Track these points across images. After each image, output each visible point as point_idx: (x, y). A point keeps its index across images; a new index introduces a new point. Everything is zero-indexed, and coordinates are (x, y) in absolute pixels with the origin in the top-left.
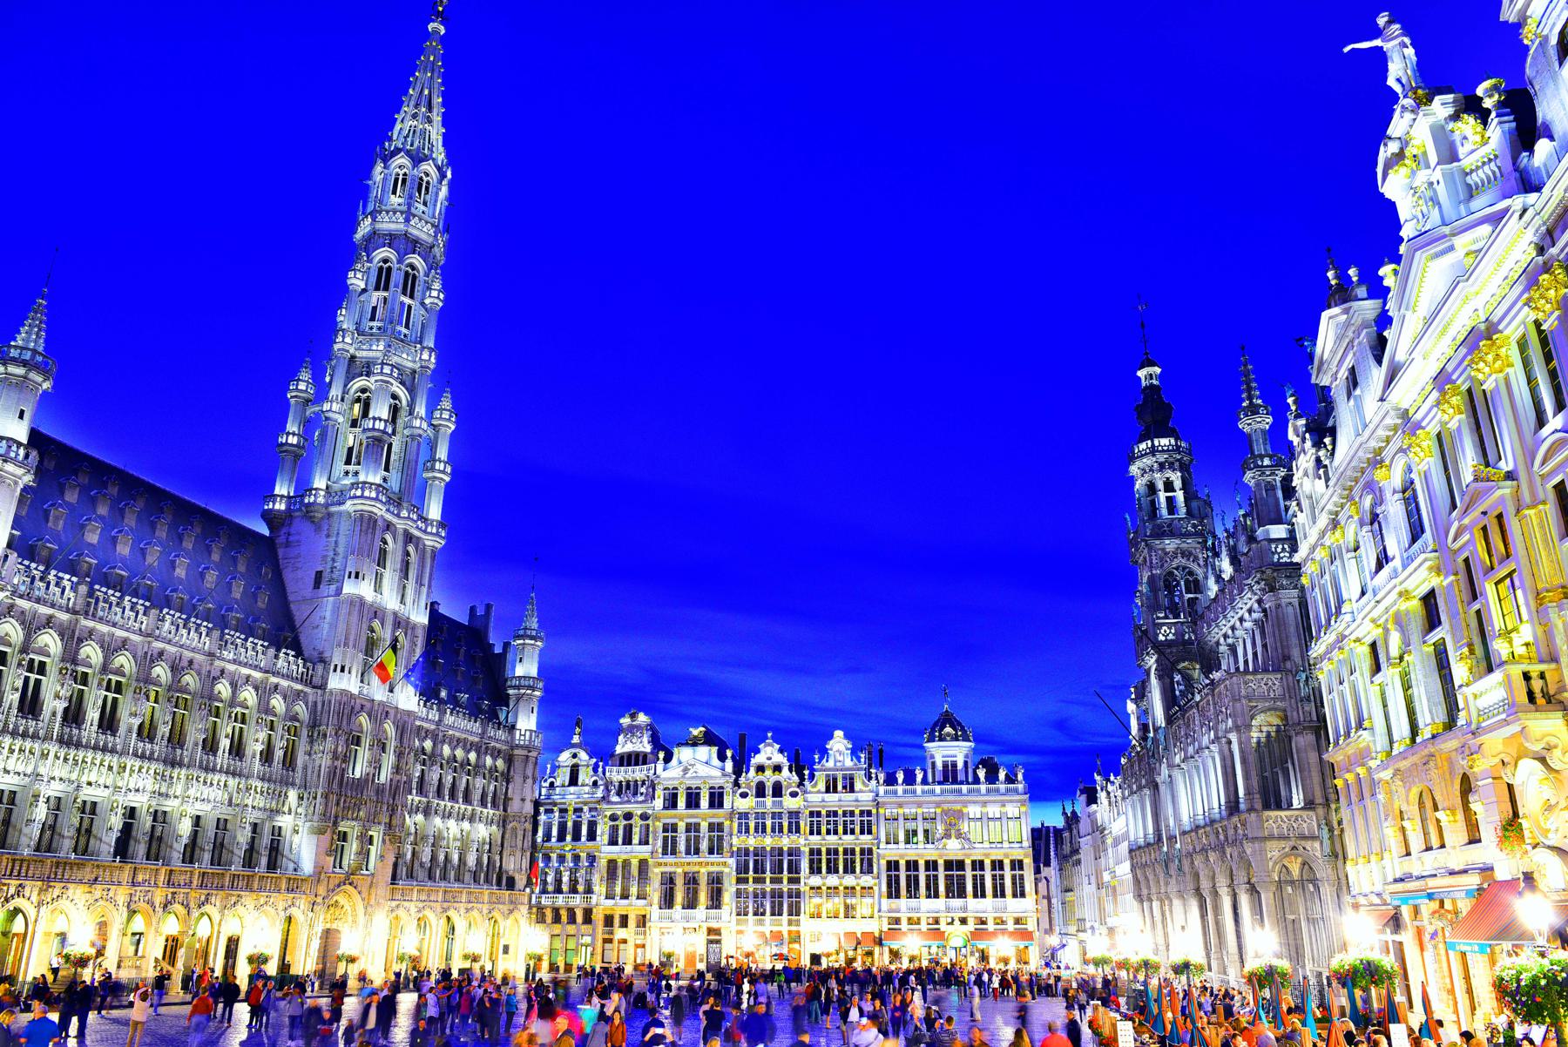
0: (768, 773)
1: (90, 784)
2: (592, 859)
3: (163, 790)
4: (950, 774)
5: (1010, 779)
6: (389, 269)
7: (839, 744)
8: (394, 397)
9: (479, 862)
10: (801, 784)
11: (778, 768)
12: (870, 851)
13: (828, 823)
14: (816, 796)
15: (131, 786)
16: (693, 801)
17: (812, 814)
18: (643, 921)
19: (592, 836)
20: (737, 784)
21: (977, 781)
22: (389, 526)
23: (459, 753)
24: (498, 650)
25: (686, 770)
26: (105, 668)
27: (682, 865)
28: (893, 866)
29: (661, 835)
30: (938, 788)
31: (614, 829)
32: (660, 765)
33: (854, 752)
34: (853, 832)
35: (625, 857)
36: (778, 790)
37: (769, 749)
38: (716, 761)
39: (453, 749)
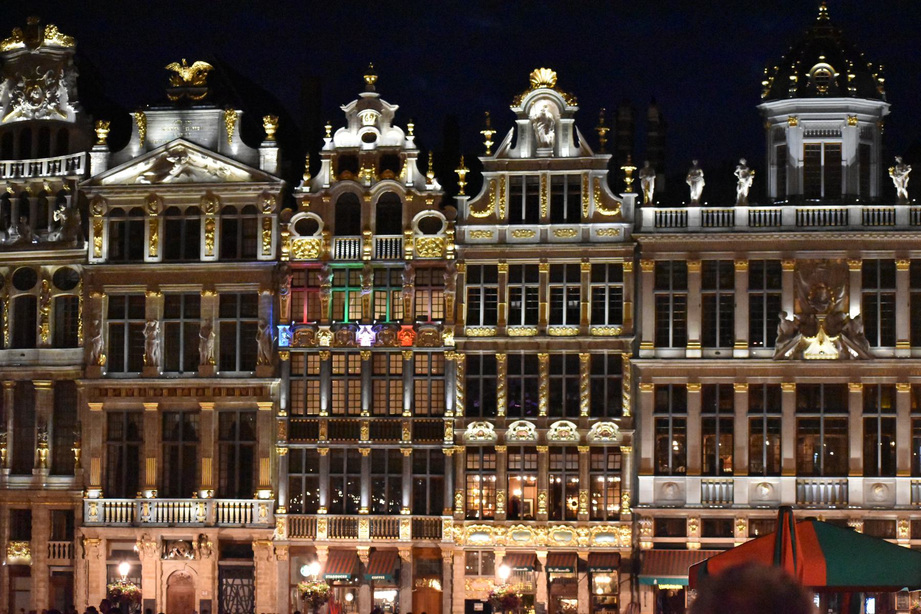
0: (366, 174)
4: (823, 177)
7: (542, 100)
10: (447, 201)
11: (390, 161)
12: (616, 363)
13: (515, 295)
16: (181, 242)
17: (473, 274)
18: (67, 524)
20: (289, 202)
21: (888, 195)
25: (162, 167)
27: (157, 394)
28: (671, 398)
29: (104, 324)
30: (788, 211)
32: (97, 160)
33: (585, 124)
34: (574, 318)
35: (19, 373)
36: (391, 216)
37: (368, 116)
38: (236, 146)
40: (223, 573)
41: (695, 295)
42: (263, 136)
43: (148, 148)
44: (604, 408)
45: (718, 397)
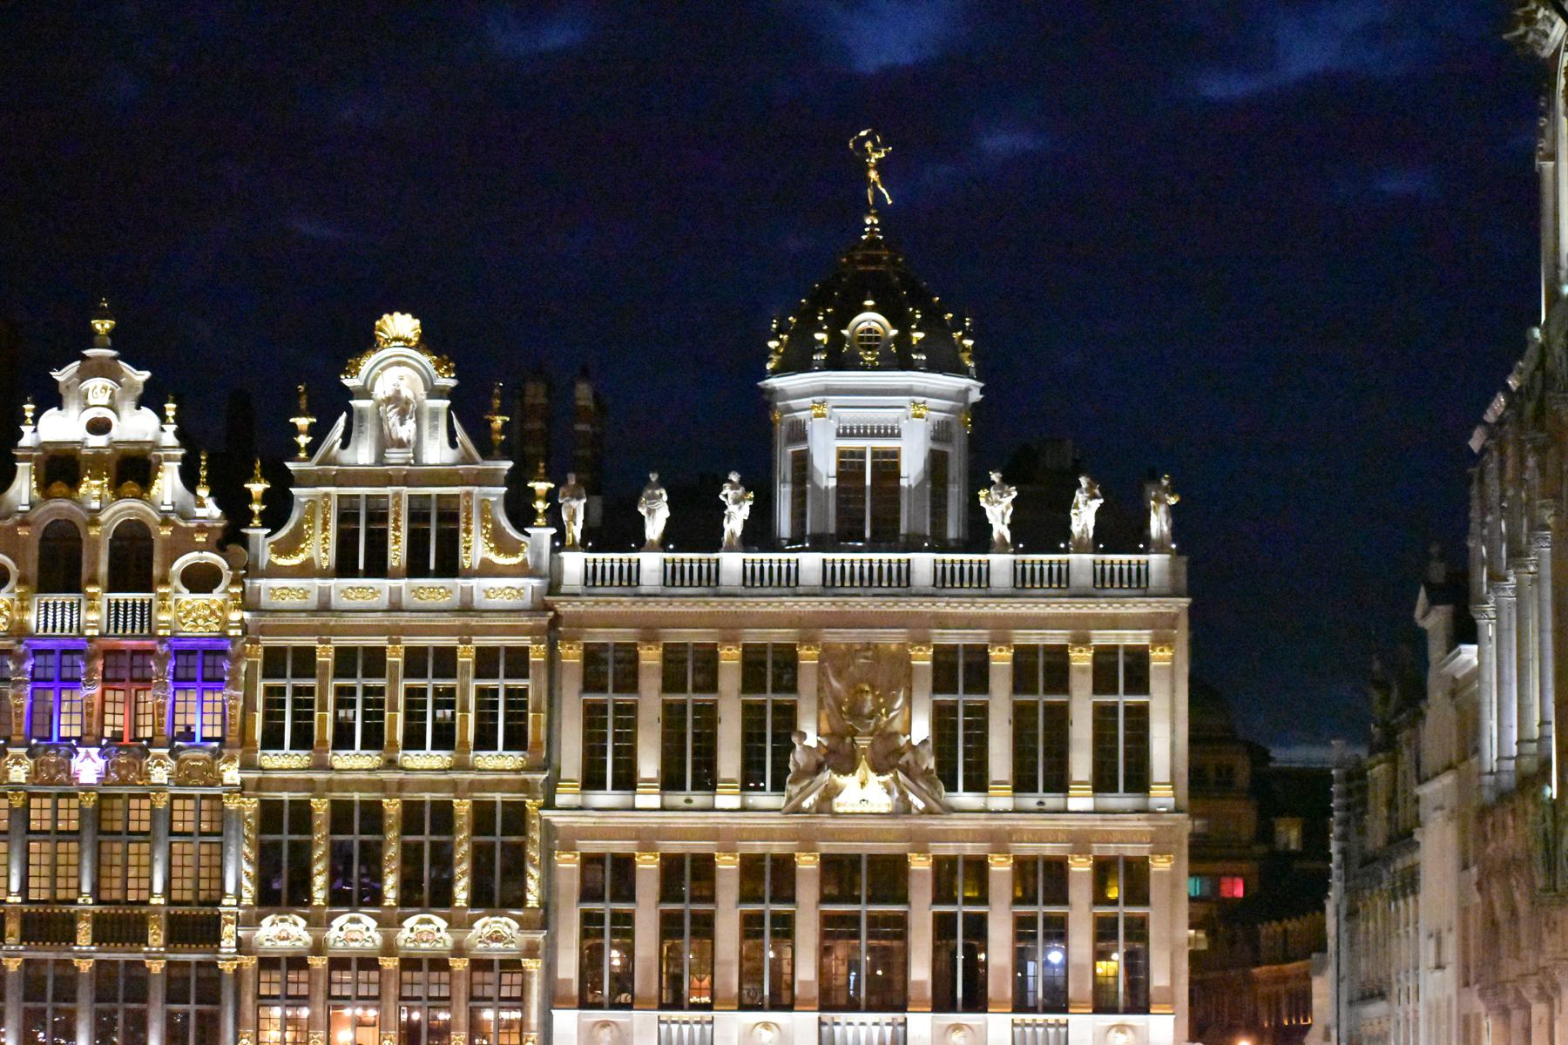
0: (92, 489)
4: (867, 507)
5: (1120, 529)
7: (397, 368)
10: (231, 537)
11: (134, 469)
12: (516, 818)
13: (345, 698)
14: (298, 582)
17: (274, 662)
21: (978, 536)
28: (610, 876)
30: (811, 563)
33: (467, 408)
34: (445, 737)
36: (134, 562)
37: (98, 389)
41: (650, 701)
45: (687, 876)
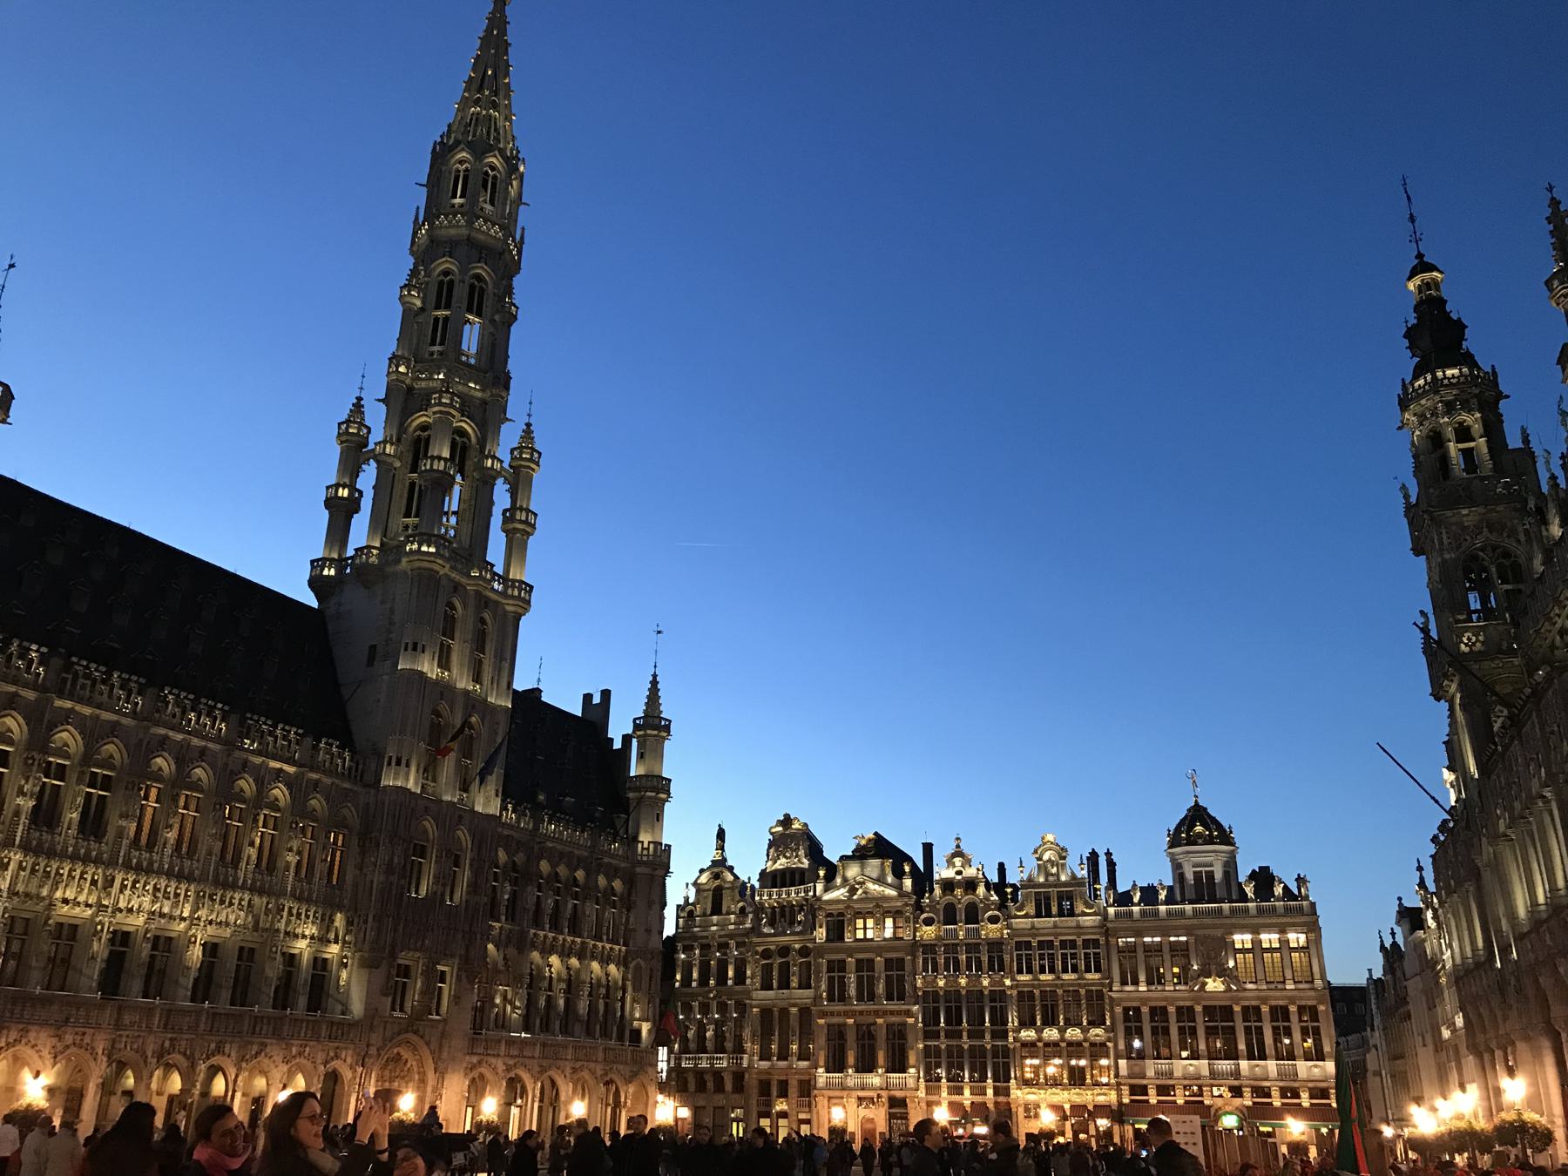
0: (958, 892)
1: (65, 901)
2: (742, 1008)
3: (166, 910)
6: (451, 282)
8: (461, 433)
9: (592, 1008)
12: (1100, 995)
13: (1042, 957)
15: (122, 905)
17: (1019, 945)
19: (740, 978)
20: (919, 908)
22: (457, 587)
23: (562, 870)
24: (617, 745)
25: (853, 891)
26: (87, 758)
30: (1188, 907)
31: (767, 970)
32: (820, 887)
34: (1075, 969)
35: (783, 1004)
36: (973, 915)
38: (890, 879)
39: (554, 866)
40: (891, 1116)
42: (904, 873)
43: (845, 880)
44: (1097, 1022)
45: (1159, 1013)
